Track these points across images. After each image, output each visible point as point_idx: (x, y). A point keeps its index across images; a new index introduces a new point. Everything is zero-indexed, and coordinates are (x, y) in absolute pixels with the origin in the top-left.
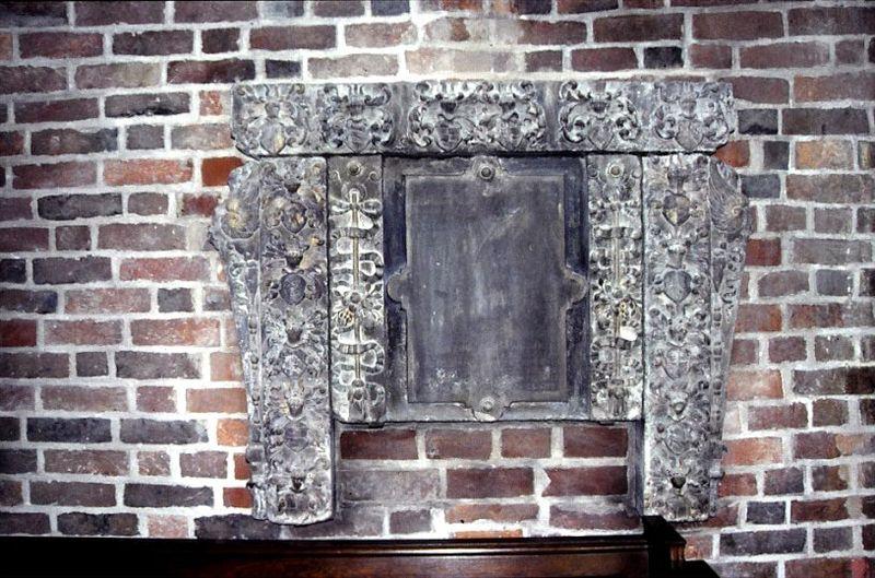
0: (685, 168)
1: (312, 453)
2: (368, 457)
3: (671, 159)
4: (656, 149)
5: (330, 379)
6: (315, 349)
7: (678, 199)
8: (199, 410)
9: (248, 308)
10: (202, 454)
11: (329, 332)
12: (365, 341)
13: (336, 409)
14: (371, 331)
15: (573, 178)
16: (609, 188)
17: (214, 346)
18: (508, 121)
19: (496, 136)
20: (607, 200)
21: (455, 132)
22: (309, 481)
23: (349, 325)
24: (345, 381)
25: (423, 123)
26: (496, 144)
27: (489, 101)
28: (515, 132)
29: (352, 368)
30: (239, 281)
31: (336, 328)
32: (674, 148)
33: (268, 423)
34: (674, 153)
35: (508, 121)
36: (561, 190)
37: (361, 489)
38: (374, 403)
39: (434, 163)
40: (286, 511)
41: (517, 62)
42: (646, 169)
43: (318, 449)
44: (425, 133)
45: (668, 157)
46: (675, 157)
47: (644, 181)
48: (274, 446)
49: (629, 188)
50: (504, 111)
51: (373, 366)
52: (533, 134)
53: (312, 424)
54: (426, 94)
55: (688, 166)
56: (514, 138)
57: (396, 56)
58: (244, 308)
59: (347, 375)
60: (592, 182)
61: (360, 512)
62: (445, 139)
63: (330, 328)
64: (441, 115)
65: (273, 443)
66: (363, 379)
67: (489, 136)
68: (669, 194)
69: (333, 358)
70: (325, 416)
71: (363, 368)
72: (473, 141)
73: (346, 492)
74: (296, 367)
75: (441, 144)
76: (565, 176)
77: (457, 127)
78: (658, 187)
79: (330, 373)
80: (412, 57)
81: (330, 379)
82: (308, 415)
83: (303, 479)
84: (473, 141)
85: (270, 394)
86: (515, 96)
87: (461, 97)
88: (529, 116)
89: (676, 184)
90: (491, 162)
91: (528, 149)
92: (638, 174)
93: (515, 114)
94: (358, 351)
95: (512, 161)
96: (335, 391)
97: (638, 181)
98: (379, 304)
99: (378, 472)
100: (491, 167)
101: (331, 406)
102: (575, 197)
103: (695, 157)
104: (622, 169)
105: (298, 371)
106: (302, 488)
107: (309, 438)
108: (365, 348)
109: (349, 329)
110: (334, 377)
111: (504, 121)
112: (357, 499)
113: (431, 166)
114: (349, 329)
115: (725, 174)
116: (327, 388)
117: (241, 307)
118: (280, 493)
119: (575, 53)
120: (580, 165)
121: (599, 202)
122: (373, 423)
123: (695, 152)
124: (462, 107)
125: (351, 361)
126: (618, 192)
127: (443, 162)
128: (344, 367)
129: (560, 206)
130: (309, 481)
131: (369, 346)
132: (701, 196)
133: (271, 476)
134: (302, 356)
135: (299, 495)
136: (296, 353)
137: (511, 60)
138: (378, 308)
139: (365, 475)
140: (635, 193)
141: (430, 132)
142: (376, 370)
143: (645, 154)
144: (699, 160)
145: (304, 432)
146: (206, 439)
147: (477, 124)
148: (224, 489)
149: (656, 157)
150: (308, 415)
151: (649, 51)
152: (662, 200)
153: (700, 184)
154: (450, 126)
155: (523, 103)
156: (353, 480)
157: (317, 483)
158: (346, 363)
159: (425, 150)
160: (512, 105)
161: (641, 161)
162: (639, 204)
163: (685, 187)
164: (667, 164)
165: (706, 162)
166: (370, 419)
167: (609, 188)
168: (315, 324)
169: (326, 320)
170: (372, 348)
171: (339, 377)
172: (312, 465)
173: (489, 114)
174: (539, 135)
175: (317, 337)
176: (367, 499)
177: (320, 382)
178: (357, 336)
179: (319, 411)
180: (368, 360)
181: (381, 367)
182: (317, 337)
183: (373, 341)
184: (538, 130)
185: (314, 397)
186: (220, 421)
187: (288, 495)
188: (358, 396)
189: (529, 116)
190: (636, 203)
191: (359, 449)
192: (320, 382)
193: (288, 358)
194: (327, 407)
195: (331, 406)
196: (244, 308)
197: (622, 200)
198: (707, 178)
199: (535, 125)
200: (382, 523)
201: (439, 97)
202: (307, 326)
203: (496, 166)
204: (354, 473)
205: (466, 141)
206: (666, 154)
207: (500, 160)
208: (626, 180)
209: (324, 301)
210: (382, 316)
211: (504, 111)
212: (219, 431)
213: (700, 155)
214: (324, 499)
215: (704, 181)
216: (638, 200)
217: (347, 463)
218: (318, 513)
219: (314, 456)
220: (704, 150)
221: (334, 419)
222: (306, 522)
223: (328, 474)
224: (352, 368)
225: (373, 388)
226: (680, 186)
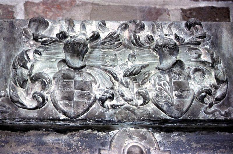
18: (169, 71)
19: (151, 95)
21: (84, 87)
25: (34, 71)
26: (151, 107)
27: (137, 43)
28: (181, 87)
35: (169, 71)
39: (51, 138)
44: (37, 87)
50: (162, 57)
52: (209, 93)
54: (43, 32)
56: (179, 96)
57: (13, 7)
62: (68, 98)
64: (64, 61)
67: (139, 94)
72: (114, 102)
75: (61, 104)
77: (89, 79)
80: (34, 9)
84: (114, 102)
86: (177, 37)
87: (95, 37)
88: (201, 66)
90: (143, 137)
91: (202, 116)
93: (179, 63)
95: (175, 136)
100: (142, 144)
111: (162, 70)
113: (43, 144)
124: (97, 53)
127: (65, 137)
141: (44, 86)
147: (120, 77)
154: (78, 78)
155: (190, 49)
159: (34, 114)
160: (174, 49)
173: (138, 63)
174: (218, 94)
184: (216, 88)
189: (201, 66)
199: (210, 81)
201: (62, 36)
203: (150, 142)
205: (102, 101)
207: (157, 135)
211: (162, 57)
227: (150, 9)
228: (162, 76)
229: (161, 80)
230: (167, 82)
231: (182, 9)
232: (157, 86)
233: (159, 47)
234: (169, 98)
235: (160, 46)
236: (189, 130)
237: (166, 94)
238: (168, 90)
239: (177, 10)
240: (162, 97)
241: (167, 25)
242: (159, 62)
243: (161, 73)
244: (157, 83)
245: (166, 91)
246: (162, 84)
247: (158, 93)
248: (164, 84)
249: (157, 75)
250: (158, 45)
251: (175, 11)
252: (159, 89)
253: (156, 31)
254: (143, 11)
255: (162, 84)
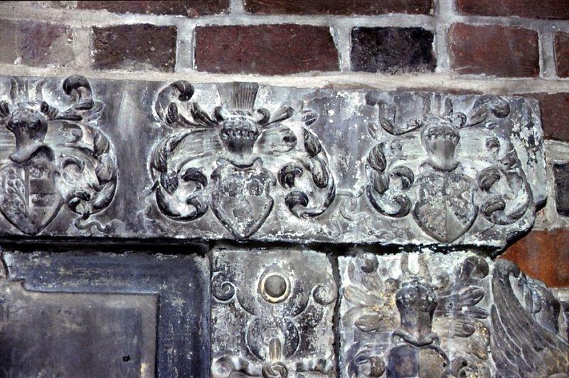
0: (435, 282)
3: (404, 262)
4: (371, 239)
7: (422, 356)
15: (178, 302)
16: (259, 327)
18: (25, 163)
20: (254, 354)
28: (41, 189)
32: (411, 236)
34: (411, 248)
35: (25, 163)
36: (149, 330)
41: (76, 46)
42: (346, 282)
45: (399, 256)
46: (413, 257)
47: (342, 312)
49: (307, 328)
50: (20, 141)
52: (84, 197)
55: (443, 278)
56: (38, 203)
60: (220, 312)
68: (401, 343)
76: (159, 298)
78: (375, 327)
86: (45, 108)
88: (78, 156)
89: (414, 321)
91: (72, 231)
92: (327, 294)
93: (45, 150)
95: (35, 258)
97: (328, 311)
102: (180, 345)
103: (460, 258)
104: (291, 280)
111: (17, 163)
115: (529, 298)
119: (202, 34)
120: (197, 271)
121: (235, 360)
123: (461, 247)
126: (281, 337)
129: (144, 367)
132: (475, 349)
137: (63, 41)
140: (322, 340)
143: (344, 249)
144: (467, 266)
149: (370, 256)
151: (362, 36)
152: (383, 356)
153: (471, 319)
155: (66, 126)
160: (39, 128)
161: (335, 265)
162: (330, 364)
163: (439, 326)
164: (396, 273)
165: (483, 270)
167: (259, 327)
174: (100, 198)
184: (97, 190)
189: (78, 156)
190: (323, 362)
197: (289, 355)
198: (487, 306)
199: (90, 177)
206: (393, 249)
208: (302, 307)
211: (20, 141)
213: (471, 254)
215: (480, 314)
216: (328, 354)
220: (479, 243)
226: (426, 323)
227: (40, 26)
228: (15, 170)
229: (13, 178)
230: (22, 180)
231: (94, 28)
232: (7, 186)
233: (13, 126)
234: (22, 205)
235: (14, 124)
236: (57, 249)
237: (18, 199)
238: (21, 192)
239: (84, 29)
240: (12, 203)
241: (36, 83)
242: (15, 145)
243: (14, 166)
244: (6, 181)
245: (19, 195)
246: (14, 183)
247: (7, 197)
248: (16, 184)
249: (8, 169)
250: (13, 123)
251: (82, 32)
252: (9, 189)
253: (17, 93)
254: (26, 30)
255: (14, 183)
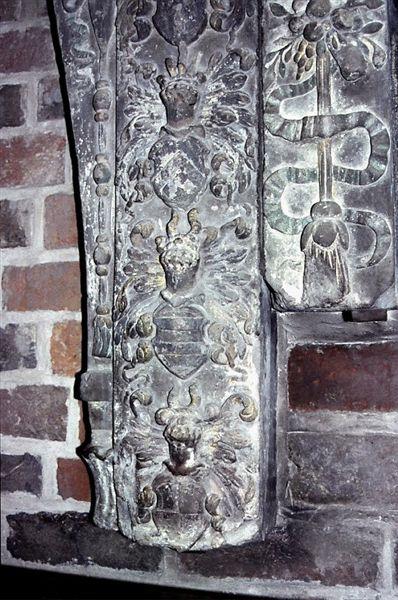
1: (215, 382)
2: (349, 405)
5: (261, 205)
6: (227, 135)
8: (25, 306)
9: (95, 72)
10: (24, 390)
11: (260, 97)
12: (338, 105)
13: (273, 277)
14: (356, 88)
17: (54, 183)
22: (207, 449)
23: (305, 77)
24: (295, 209)
29: (313, 175)
30: (80, 22)
31: (276, 87)
33: (122, 310)
37: (332, 477)
38: (365, 259)
40: (155, 516)
43: (231, 372)
48: (133, 364)
51: (362, 167)
53: (217, 312)
58: (88, 72)
59: (300, 195)
61: (328, 528)
63: (262, 87)
65: (131, 355)
66: (340, 201)
69: (267, 156)
70: (248, 294)
71: (342, 175)
73: (297, 482)
74: (184, 178)
79: (261, 188)
81: (261, 205)
82: (209, 290)
83: (192, 442)
85: (128, 245)
94: (327, 129)
96: (271, 233)
98: (376, 21)
99: (372, 440)
101: (263, 271)
105: (189, 187)
106: (189, 463)
107: (208, 344)
108: (342, 123)
109: (306, 86)
110: (270, 199)
112: (324, 500)
114: (306, 86)
116: (254, 227)
117: (80, 72)
118: (143, 472)
122: (363, 309)
125: (310, 159)
128: (295, 175)
130: (207, 449)
131: (352, 120)
133: (125, 433)
134: (195, 150)
135: (181, 479)
136: (183, 146)
138: (373, 29)
139: (342, 446)
142: (372, 176)
145: (197, 331)
146: (31, 362)
148: (60, 460)
150: (209, 290)
156: (314, 456)
157: (224, 452)
158: (297, 165)
166: (355, 298)
168: (226, 81)
169: (253, 72)
170: (361, 124)
171: (284, 198)
172: (214, 411)
175: (232, 110)
176: (343, 500)
177: (238, 211)
178: (323, 97)
179: (234, 281)
180: (350, 152)
181: (384, 169)
182: (232, 110)
183: (363, 108)
185: (223, 246)
186: (57, 326)
187: (158, 479)
188: (324, 237)
191: (331, 386)
192: (238, 211)
193: (167, 159)
194: (254, 271)
195: (263, 271)
196: (88, 72)
200: (376, 557)
202: (211, 87)
204: (318, 440)
209: (248, 30)
210: (382, 46)
212: (55, 345)
214: (241, 492)
217: (303, 419)
218: (226, 526)
219: (223, 387)
221: (272, 298)
222: (198, 546)
223: (253, 434)
224: (313, 175)
225: (361, 221)
